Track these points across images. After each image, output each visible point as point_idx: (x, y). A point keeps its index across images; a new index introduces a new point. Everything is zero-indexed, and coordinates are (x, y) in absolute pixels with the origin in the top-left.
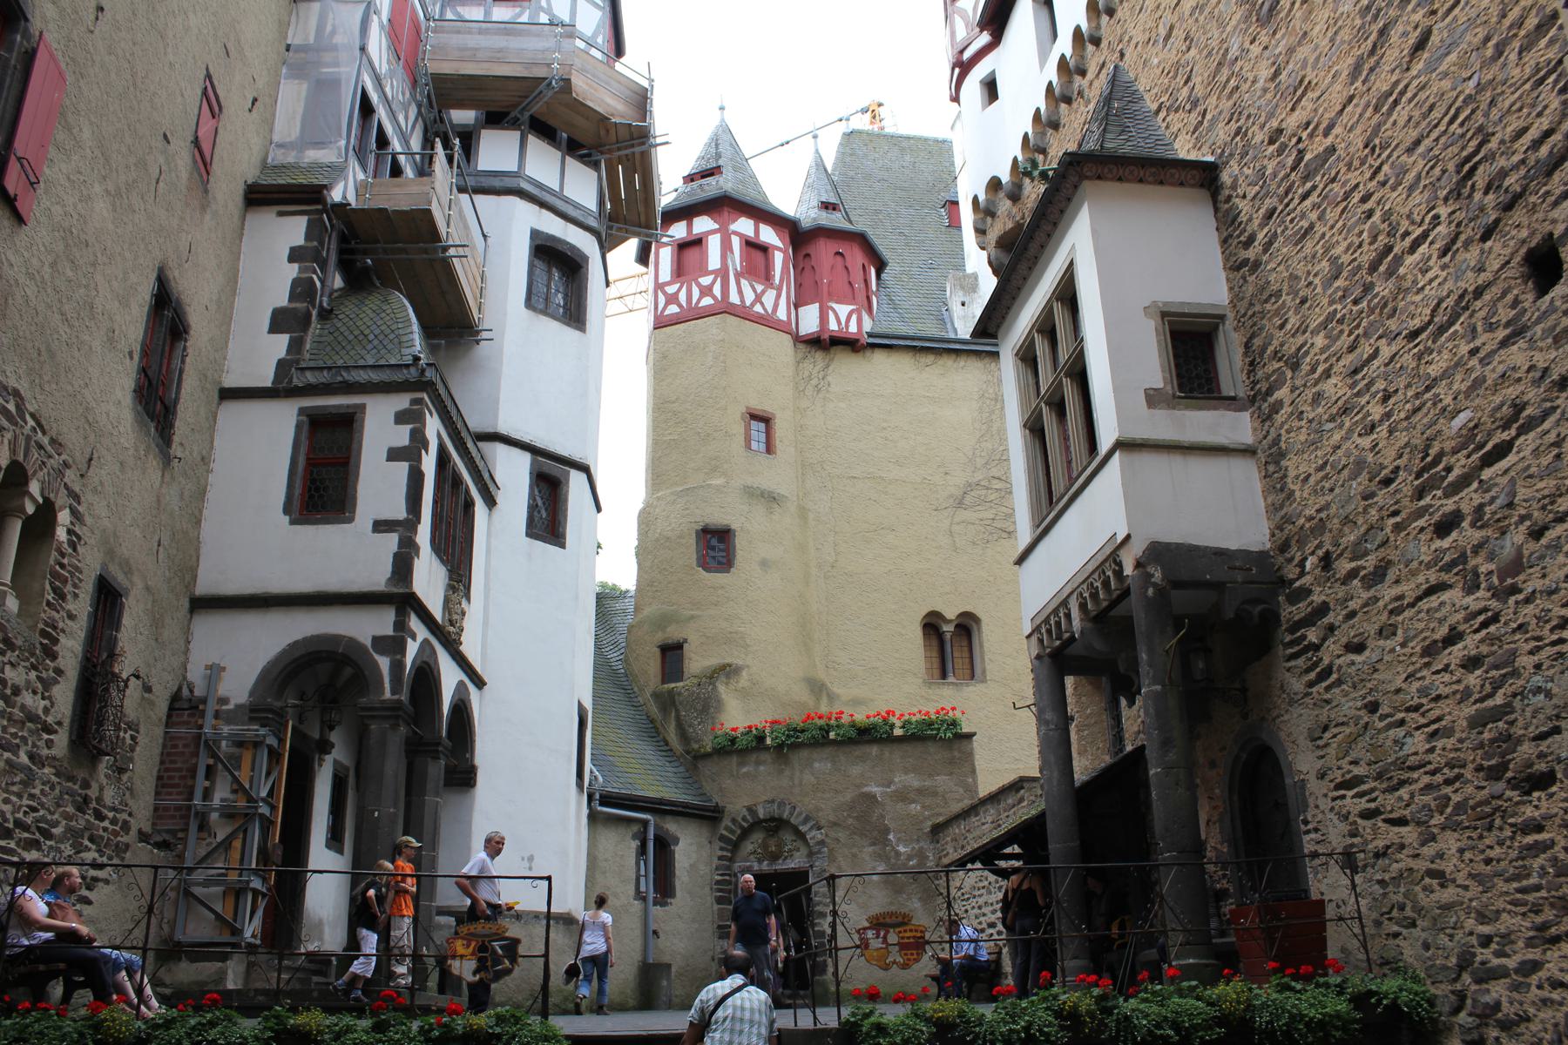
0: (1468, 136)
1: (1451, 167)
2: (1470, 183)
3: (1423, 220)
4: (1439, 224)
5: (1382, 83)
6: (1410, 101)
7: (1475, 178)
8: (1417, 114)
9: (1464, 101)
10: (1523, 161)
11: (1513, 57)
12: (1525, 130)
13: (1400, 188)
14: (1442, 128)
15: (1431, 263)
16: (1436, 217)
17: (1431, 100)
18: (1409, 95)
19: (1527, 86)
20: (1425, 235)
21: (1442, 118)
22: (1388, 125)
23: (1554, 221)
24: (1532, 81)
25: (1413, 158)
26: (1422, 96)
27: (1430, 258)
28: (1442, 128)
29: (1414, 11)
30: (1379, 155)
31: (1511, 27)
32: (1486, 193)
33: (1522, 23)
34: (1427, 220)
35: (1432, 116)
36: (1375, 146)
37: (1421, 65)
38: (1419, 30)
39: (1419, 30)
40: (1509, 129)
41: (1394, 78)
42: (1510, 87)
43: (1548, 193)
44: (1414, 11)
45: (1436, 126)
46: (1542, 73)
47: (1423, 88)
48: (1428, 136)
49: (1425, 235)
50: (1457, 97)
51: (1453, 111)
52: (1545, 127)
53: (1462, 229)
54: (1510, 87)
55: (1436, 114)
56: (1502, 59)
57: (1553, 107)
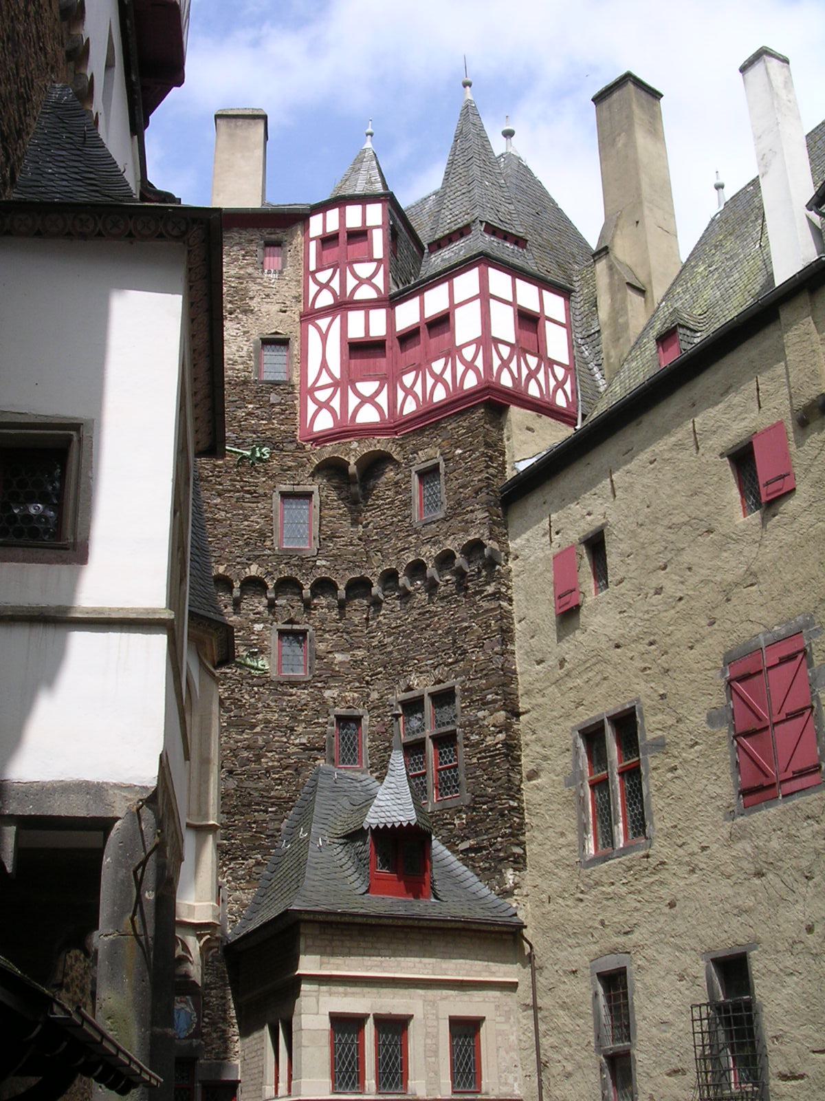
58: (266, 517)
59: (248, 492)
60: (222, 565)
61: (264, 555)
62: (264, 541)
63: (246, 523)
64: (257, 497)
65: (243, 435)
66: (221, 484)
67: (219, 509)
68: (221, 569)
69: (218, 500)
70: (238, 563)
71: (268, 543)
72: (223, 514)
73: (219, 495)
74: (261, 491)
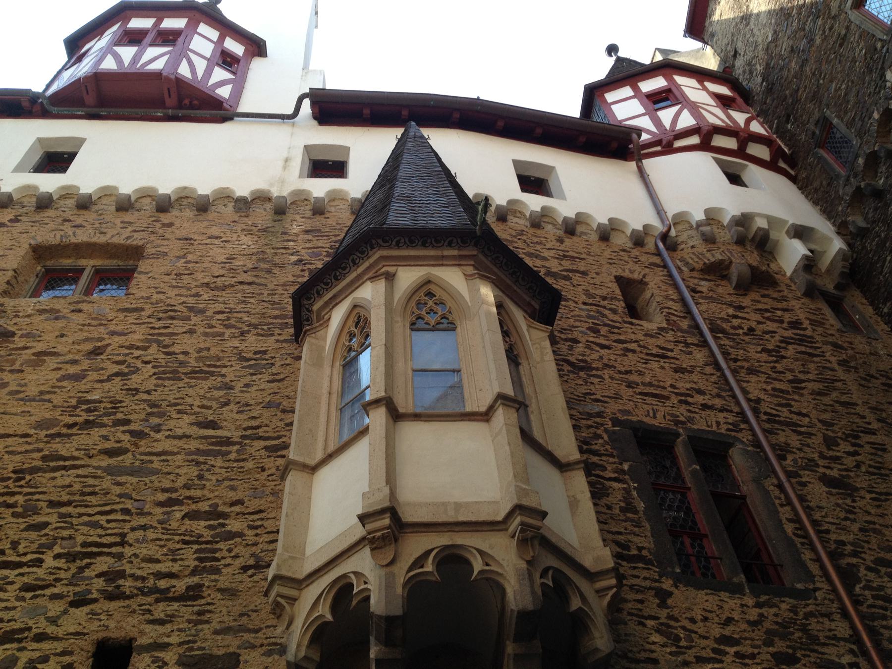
0: (109, 532)
1: (80, 539)
2: (88, 561)
3: (25, 554)
4: (38, 567)
5: (63, 448)
6: (78, 476)
7: (93, 561)
8: (77, 487)
9: (122, 510)
10: (143, 579)
11: (178, 515)
12: (158, 561)
13: (21, 520)
14: (90, 511)
15: (9, 587)
16: (41, 561)
17: (97, 489)
18: (80, 472)
19: (177, 538)
20: (20, 565)
21: (96, 506)
22: (48, 475)
23: (142, 633)
24: (182, 537)
25: (51, 511)
26: (91, 481)
27: (12, 583)
28: (90, 511)
29: (123, 432)
30: (21, 486)
31: (189, 498)
32: (98, 576)
33: (197, 502)
34: (29, 557)
35: (88, 498)
36: (24, 478)
37: (104, 464)
38: (119, 445)
39: (119, 445)
40: (144, 551)
41: (76, 454)
42: (163, 528)
43: (149, 611)
44: (123, 432)
45: (86, 506)
46: (192, 539)
47: (95, 477)
48: (75, 507)
49: (20, 565)
50: (118, 503)
51: (108, 508)
52: (174, 570)
53: (58, 584)
54: (163, 528)
55: (93, 500)
56: (168, 509)
57: (186, 563)
58: (861, 36)
59: (841, 45)
60: (873, 112)
61: (885, 56)
62: (876, 49)
63: (857, 63)
64: (843, 40)
65: (807, 28)
66: (825, 76)
67: (840, 88)
68: (876, 116)
69: (834, 85)
70: (880, 92)
71: (879, 45)
72: (844, 86)
73: (831, 81)
74: (843, 32)
